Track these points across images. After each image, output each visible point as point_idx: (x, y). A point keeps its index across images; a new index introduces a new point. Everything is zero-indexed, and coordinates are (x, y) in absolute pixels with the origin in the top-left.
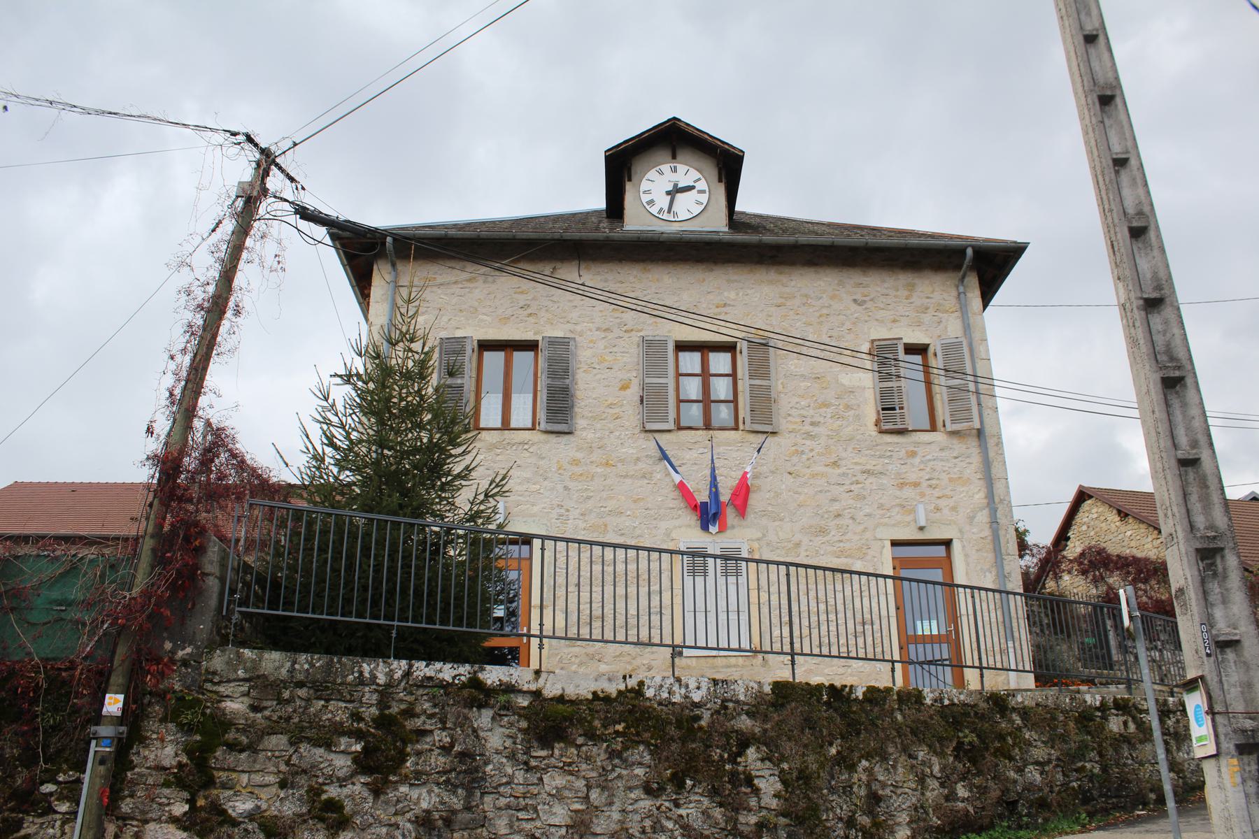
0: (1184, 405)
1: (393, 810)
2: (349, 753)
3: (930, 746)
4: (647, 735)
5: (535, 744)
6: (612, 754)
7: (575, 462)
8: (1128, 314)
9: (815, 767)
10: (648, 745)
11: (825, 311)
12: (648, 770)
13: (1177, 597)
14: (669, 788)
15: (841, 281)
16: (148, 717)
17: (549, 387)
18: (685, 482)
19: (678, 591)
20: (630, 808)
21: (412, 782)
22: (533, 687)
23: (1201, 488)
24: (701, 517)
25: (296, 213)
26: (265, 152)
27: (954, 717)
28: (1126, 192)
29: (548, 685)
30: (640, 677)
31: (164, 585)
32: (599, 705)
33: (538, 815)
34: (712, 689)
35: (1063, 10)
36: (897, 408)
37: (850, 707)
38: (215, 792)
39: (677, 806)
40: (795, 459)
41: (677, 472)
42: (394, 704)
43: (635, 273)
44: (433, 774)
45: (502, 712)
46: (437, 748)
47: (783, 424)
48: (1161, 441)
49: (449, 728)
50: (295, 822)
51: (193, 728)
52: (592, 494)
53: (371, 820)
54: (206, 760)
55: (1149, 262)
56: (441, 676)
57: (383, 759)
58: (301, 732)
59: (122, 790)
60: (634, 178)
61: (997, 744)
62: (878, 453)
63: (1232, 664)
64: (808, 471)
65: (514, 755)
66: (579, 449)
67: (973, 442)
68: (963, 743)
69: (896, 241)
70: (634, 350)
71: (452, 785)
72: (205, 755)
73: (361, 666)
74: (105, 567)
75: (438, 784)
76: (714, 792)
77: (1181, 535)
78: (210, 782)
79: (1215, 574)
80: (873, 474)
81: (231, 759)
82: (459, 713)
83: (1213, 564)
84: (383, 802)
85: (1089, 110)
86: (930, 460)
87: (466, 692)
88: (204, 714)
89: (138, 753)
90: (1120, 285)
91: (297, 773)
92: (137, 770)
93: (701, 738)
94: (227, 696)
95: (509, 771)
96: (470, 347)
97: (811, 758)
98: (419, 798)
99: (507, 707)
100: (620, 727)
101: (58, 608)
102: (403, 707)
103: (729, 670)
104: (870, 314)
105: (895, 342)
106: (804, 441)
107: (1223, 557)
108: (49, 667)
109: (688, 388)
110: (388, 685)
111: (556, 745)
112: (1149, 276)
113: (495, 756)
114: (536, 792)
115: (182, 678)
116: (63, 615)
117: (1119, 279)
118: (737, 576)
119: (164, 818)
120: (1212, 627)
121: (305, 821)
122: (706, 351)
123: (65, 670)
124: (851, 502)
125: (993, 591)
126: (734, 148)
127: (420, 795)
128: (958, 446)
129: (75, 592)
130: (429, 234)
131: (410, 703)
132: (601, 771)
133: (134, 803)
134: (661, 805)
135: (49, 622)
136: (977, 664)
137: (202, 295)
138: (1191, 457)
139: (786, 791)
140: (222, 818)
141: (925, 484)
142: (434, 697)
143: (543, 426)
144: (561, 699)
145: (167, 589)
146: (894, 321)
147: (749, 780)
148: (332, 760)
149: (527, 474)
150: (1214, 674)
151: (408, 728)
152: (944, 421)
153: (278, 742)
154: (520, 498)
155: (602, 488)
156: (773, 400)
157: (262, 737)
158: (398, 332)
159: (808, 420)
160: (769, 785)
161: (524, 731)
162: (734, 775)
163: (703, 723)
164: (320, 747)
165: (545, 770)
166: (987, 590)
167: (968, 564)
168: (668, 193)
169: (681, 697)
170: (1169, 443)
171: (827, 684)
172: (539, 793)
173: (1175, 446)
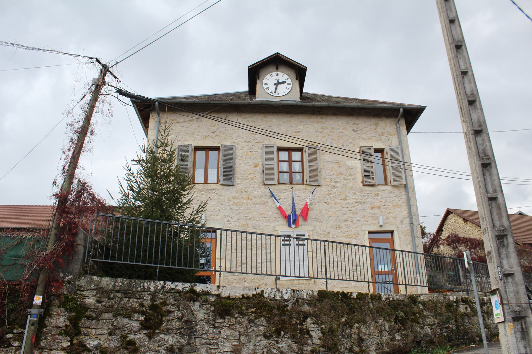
0: (491, 175)
1: (157, 345)
2: (139, 321)
3: (384, 318)
4: (265, 313)
5: (218, 317)
6: (250, 321)
7: (235, 198)
8: (468, 136)
9: (336, 326)
10: (265, 317)
11: (340, 134)
12: (265, 328)
13: (488, 255)
14: (274, 335)
15: (347, 122)
16: (53, 305)
17: (224, 166)
18: (281, 206)
19: (278, 252)
20: (258, 344)
21: (165, 333)
22: (217, 293)
23: (497, 209)
24: (288, 221)
25: (117, 92)
26: (104, 66)
27: (394, 306)
28: (467, 85)
29: (223, 292)
30: (262, 289)
31: (60, 249)
32: (244, 300)
33: (219, 347)
34: (292, 294)
35: (441, 10)
36: (371, 175)
37: (350, 301)
38: (81, 337)
39: (278, 343)
40: (328, 197)
41: (278, 202)
42: (158, 300)
43: (261, 118)
44: (174, 329)
45: (204, 303)
46: (176, 318)
47: (323, 182)
48: (481, 190)
49: (181, 310)
50: (115, 350)
51: (72, 310)
52: (242, 211)
53: (148, 349)
54: (77, 323)
55: (476, 115)
56: (178, 288)
57: (152, 323)
58: (118, 311)
59: (41, 336)
60: (260, 78)
61: (413, 317)
62: (363, 194)
63: (511, 283)
64: (333, 202)
65: (208, 321)
66: (237, 192)
67: (403, 190)
68: (398, 316)
69: (370, 105)
70: (260, 151)
71: (182, 334)
72: (77, 321)
73: (144, 284)
74: (35, 241)
75: (176, 334)
76: (293, 337)
77: (489, 229)
78: (79, 333)
79: (503, 246)
80: (360, 203)
81: (88, 323)
82: (185, 303)
83: (503, 241)
84: (153, 341)
85: (451, 51)
86: (384, 197)
87: (188, 295)
88: (77, 304)
89: (48, 321)
90: (464, 124)
91: (116, 329)
92: (48, 328)
93: (287, 314)
94: (87, 296)
95: (207, 328)
96: (191, 149)
97: (334, 323)
98: (168, 340)
99: (206, 301)
100: (253, 310)
101: (15, 259)
102: (162, 301)
103: (300, 285)
104: (360, 136)
105: (370, 147)
106: (331, 189)
107: (507, 239)
108: (10, 284)
109: (283, 166)
110: (155, 292)
111: (227, 317)
112: (476, 121)
113: (200, 322)
114: (218, 337)
115: (68, 289)
116: (17, 262)
117: (464, 122)
118: (303, 246)
119: (59, 348)
120: (502, 268)
121: (119, 350)
122: (290, 151)
123: (17, 285)
125: (411, 252)
126: (302, 65)
127: (169, 338)
128: (396, 191)
129: (22, 252)
130: (173, 101)
131: (165, 299)
132: (245, 328)
133: (46, 342)
134: (271, 343)
135: (11, 265)
136: (404, 283)
137: (77, 126)
138: (493, 197)
139: (324, 337)
140: (84, 348)
141: (382, 207)
142: (175, 297)
143: (222, 182)
144: (228, 298)
145: (61, 251)
146: (370, 139)
147: (308, 332)
148: (131, 324)
149: (215, 203)
150: (503, 287)
151: (164, 310)
152: (390, 181)
153: (108, 316)
154: (211, 213)
155: (246, 209)
156: (319, 172)
157: (101, 314)
158: (160, 142)
159: (333, 180)
160: (316, 334)
161: (213, 311)
162: (302, 329)
163: (289, 308)
164: (126, 318)
165: (222, 328)
166: (408, 252)
167: (400, 241)
168: (275, 84)
169: (279, 297)
170: (484, 191)
171: (341, 292)
172: (219, 338)
173: (487, 192)
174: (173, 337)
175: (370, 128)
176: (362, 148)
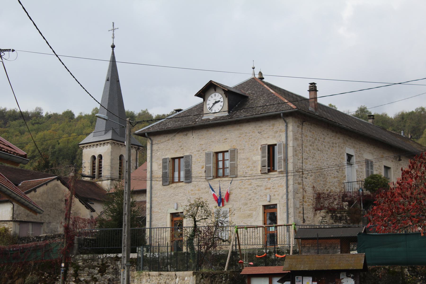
1: (104, 278)
7: (192, 190)
11: (251, 137)
15: (255, 126)
38: (79, 277)
40: (241, 184)
56: (111, 256)
64: (243, 187)
66: (193, 187)
80: (259, 186)
81: (80, 272)
86: (273, 181)
88: (76, 265)
105: (266, 145)
110: (103, 258)
115: (73, 260)
124: (254, 195)
141: (272, 188)
146: (268, 137)
149: (182, 195)
153: (87, 269)
159: (244, 172)
167: (280, 211)
174: (110, 275)
175: (269, 129)
176: (262, 146)
